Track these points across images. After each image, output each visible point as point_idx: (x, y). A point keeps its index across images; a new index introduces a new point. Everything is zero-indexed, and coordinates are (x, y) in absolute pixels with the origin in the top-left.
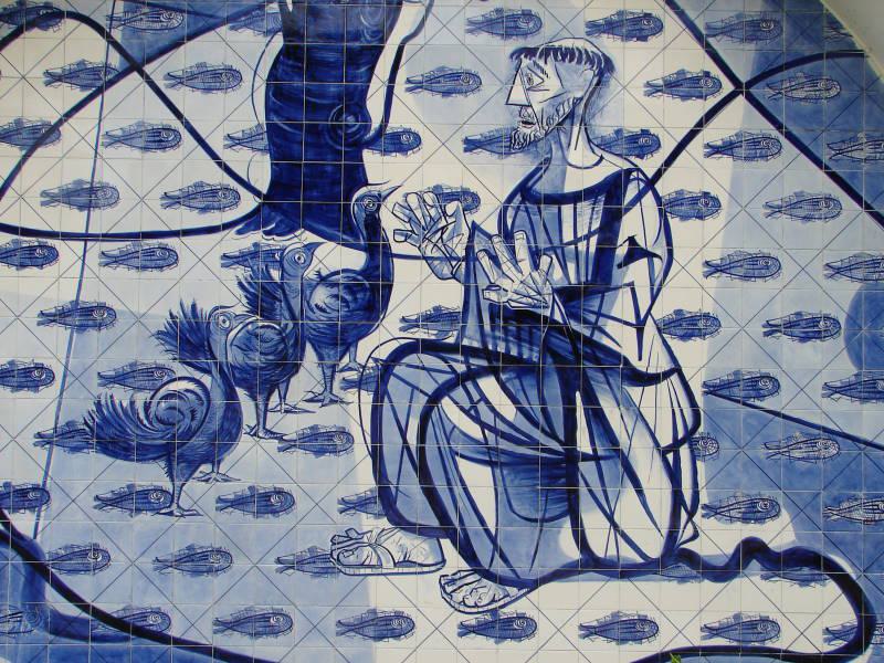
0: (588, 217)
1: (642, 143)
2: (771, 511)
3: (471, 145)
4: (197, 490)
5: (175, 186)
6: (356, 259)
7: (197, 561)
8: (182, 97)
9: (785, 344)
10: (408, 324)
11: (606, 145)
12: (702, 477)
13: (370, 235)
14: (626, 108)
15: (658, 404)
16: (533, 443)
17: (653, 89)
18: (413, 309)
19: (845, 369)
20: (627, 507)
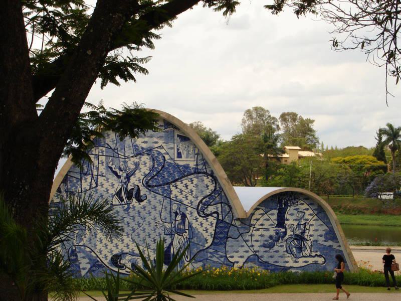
0: (303, 226)
1: (307, 220)
3: (294, 220)
4: (271, 250)
5: (269, 224)
6: (284, 230)
7: (271, 257)
8: (270, 216)
9: (319, 237)
12: (312, 249)
13: (285, 228)
14: (307, 217)
15: (309, 242)
19: (324, 239)
20: (306, 251)
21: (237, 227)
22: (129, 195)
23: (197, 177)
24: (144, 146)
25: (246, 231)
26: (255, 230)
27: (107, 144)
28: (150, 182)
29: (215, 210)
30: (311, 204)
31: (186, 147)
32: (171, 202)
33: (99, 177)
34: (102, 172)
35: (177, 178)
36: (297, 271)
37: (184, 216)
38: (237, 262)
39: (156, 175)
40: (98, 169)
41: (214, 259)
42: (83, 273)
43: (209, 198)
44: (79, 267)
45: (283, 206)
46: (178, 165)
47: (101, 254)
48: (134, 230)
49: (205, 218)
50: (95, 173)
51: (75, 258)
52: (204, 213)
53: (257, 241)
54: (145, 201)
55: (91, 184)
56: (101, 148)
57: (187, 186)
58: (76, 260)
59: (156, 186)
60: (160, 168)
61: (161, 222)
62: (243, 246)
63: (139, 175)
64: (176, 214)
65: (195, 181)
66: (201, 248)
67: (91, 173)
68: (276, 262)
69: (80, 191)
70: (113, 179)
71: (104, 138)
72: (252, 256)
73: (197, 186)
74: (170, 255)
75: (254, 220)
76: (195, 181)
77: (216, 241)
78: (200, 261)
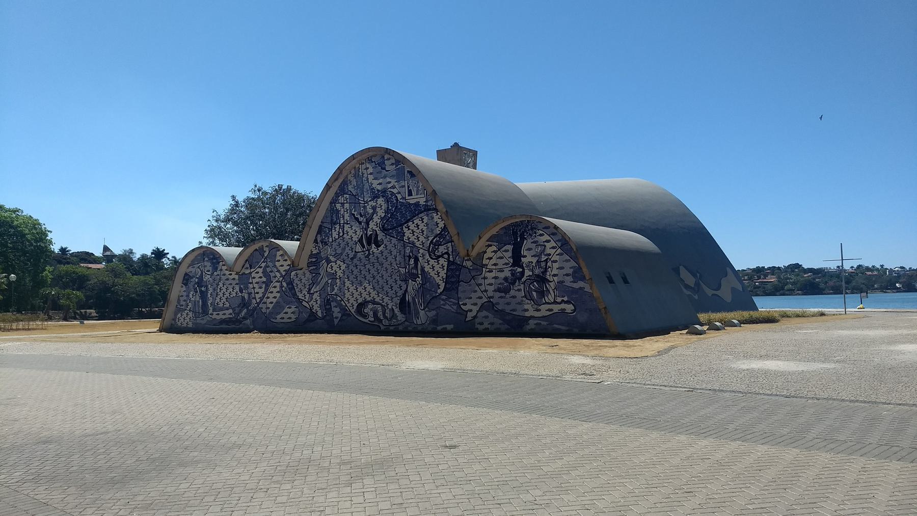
2: (565, 297)
3: (532, 256)
6: (521, 270)
7: (508, 304)
10: (527, 277)
11: (546, 255)
13: (522, 267)
14: (548, 251)
16: (539, 289)
17: (550, 248)
18: (527, 275)
19: (572, 280)
21: (469, 269)
22: (369, 244)
23: (427, 215)
24: (379, 187)
25: (478, 273)
26: (488, 272)
27: (350, 191)
28: (386, 226)
29: (446, 251)
30: (554, 234)
31: (415, 183)
32: (404, 245)
35: (409, 218)
36: (539, 322)
37: (416, 260)
38: (471, 311)
39: (390, 218)
41: (447, 307)
42: (336, 321)
43: (439, 237)
45: (519, 240)
46: (410, 204)
47: (349, 303)
48: (374, 277)
49: (436, 261)
50: (342, 222)
52: (435, 254)
53: (491, 284)
54: (382, 246)
57: (418, 226)
59: (390, 229)
60: (393, 209)
61: (396, 268)
62: (475, 291)
63: (376, 219)
64: (410, 257)
65: (426, 219)
66: (434, 295)
68: (514, 310)
70: (356, 226)
72: (485, 304)
73: (427, 224)
74: (405, 303)
75: (486, 259)
76: (426, 219)
77: (447, 286)
78: (433, 310)
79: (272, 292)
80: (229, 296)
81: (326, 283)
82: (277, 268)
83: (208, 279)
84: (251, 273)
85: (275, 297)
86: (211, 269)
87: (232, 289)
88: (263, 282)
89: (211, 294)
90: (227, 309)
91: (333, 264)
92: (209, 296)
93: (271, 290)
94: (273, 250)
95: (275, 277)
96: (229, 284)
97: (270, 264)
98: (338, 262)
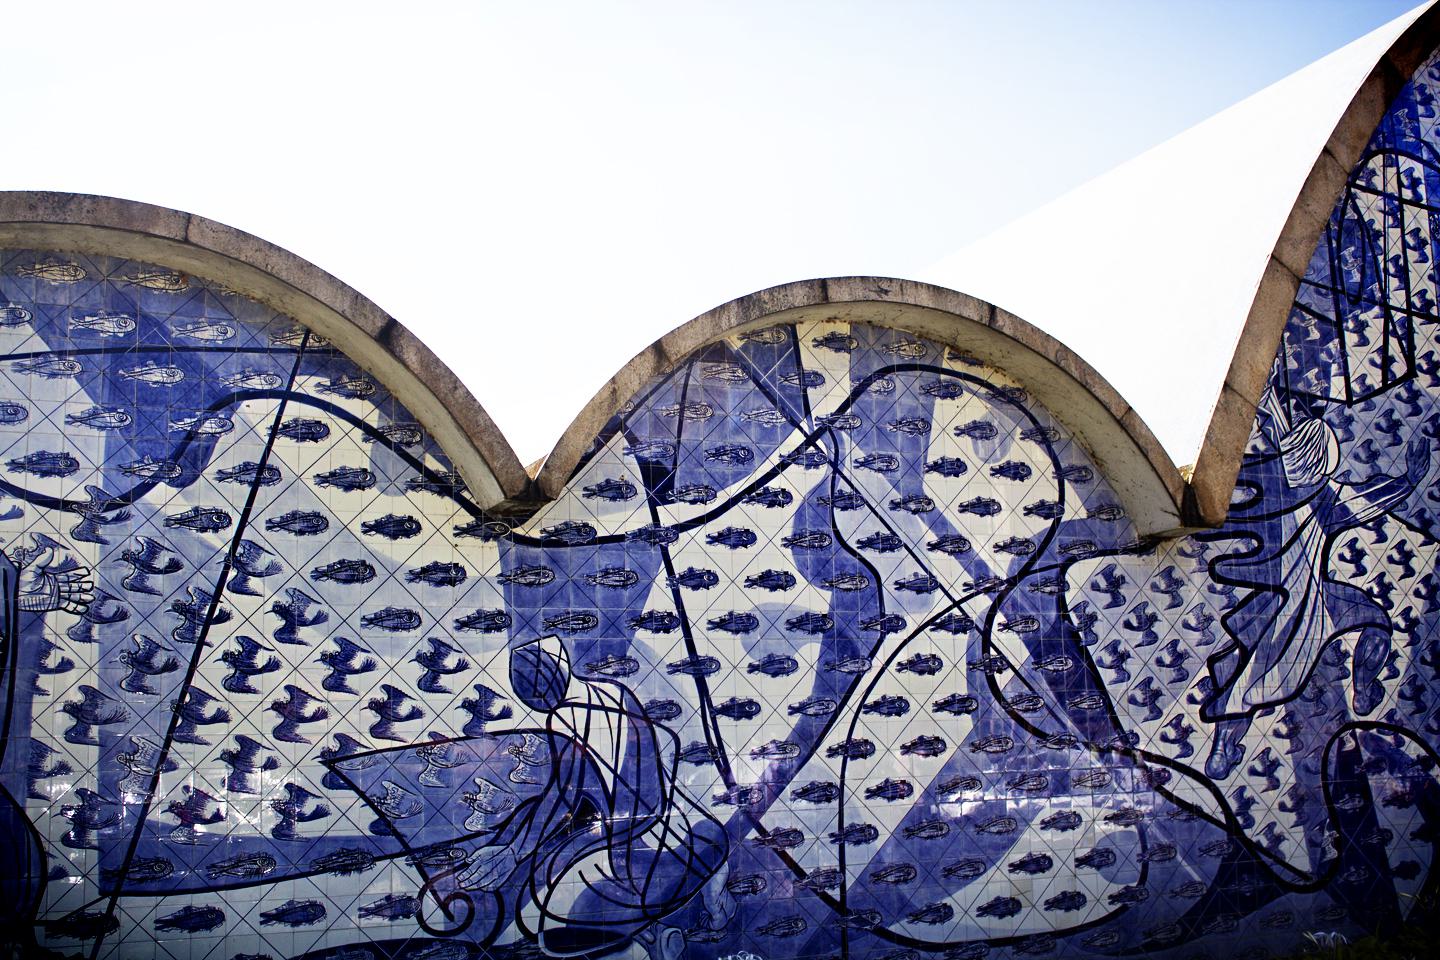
33: (1416, 321)
34: (1422, 293)
40: (1403, 274)
44: (1384, 859)
50: (1397, 299)
51: (1358, 803)
55: (1387, 362)
56: (1405, 163)
58: (1368, 812)
67: (1378, 295)
69: (1343, 397)
71: (1413, 116)
79: (895, 706)
80: (377, 731)
81: (1329, 654)
82: (938, 522)
83: (45, 542)
84: (656, 537)
85: (929, 746)
86: (91, 447)
87: (419, 671)
88: (806, 623)
89: (71, 709)
90: (348, 858)
91: (1365, 537)
92: (49, 721)
93: (888, 687)
94: (899, 380)
95: (925, 585)
96: (376, 620)
97: (872, 484)
98: (1391, 527)
